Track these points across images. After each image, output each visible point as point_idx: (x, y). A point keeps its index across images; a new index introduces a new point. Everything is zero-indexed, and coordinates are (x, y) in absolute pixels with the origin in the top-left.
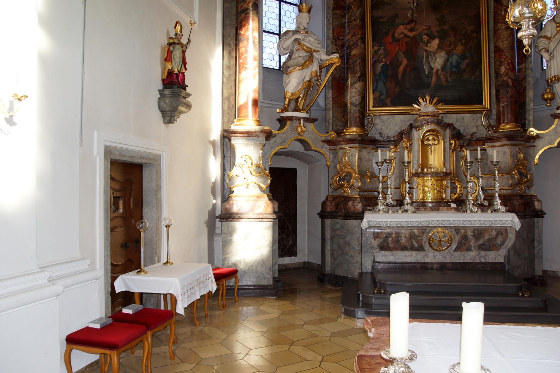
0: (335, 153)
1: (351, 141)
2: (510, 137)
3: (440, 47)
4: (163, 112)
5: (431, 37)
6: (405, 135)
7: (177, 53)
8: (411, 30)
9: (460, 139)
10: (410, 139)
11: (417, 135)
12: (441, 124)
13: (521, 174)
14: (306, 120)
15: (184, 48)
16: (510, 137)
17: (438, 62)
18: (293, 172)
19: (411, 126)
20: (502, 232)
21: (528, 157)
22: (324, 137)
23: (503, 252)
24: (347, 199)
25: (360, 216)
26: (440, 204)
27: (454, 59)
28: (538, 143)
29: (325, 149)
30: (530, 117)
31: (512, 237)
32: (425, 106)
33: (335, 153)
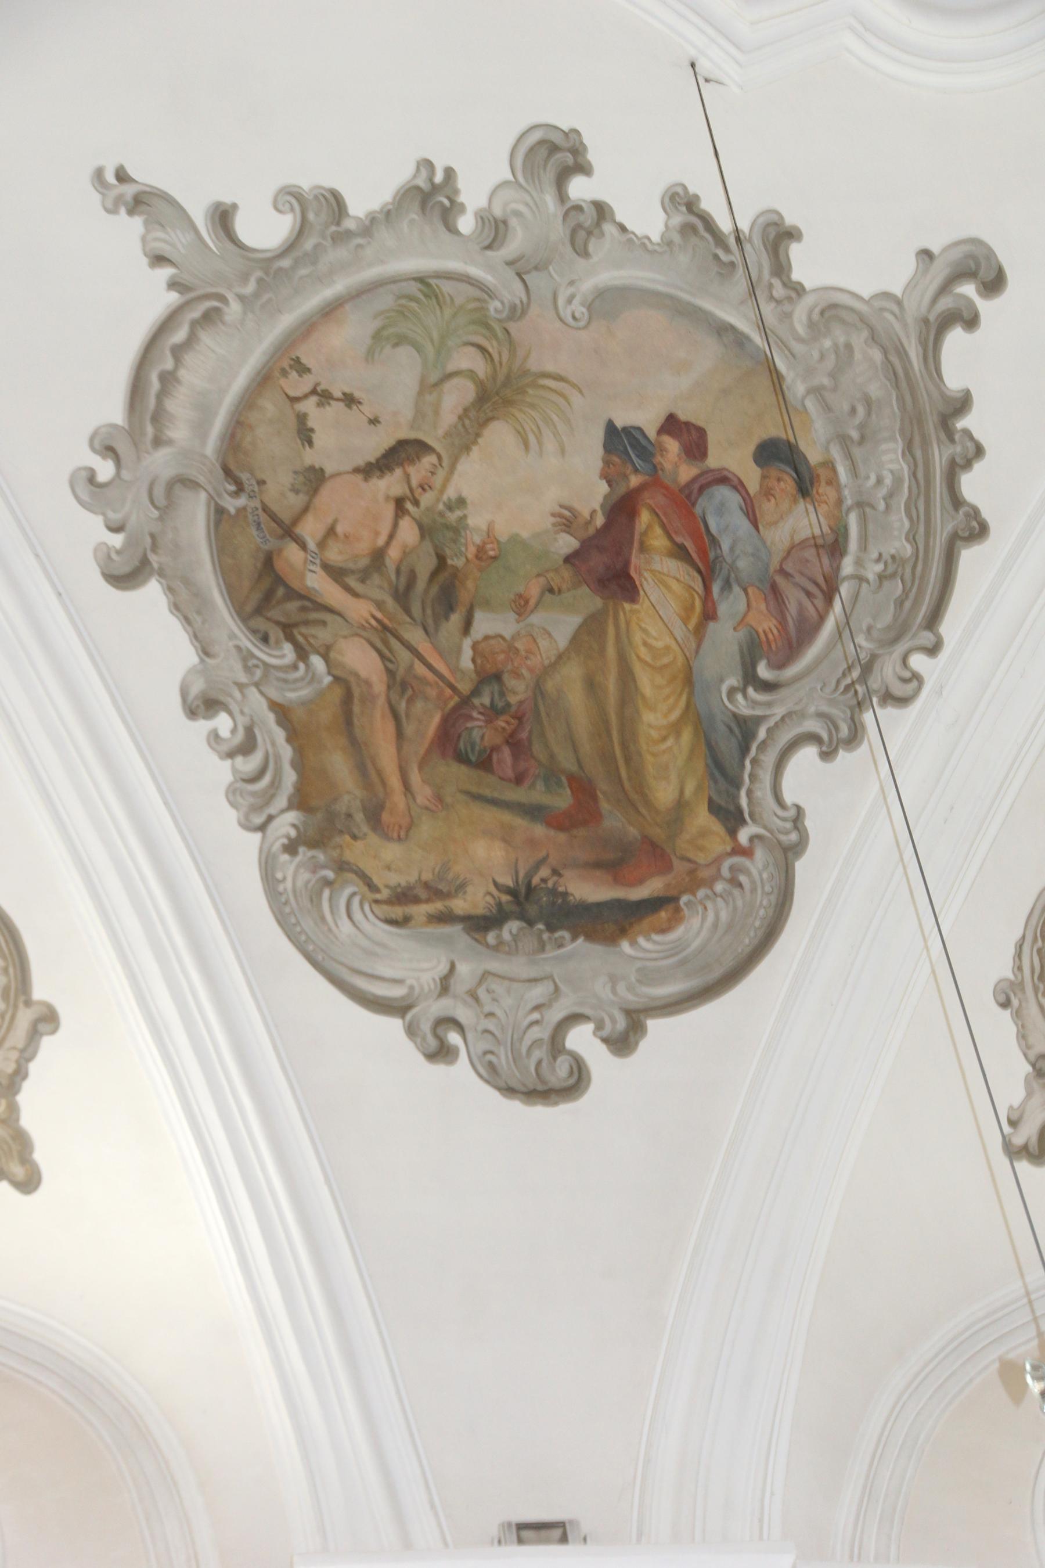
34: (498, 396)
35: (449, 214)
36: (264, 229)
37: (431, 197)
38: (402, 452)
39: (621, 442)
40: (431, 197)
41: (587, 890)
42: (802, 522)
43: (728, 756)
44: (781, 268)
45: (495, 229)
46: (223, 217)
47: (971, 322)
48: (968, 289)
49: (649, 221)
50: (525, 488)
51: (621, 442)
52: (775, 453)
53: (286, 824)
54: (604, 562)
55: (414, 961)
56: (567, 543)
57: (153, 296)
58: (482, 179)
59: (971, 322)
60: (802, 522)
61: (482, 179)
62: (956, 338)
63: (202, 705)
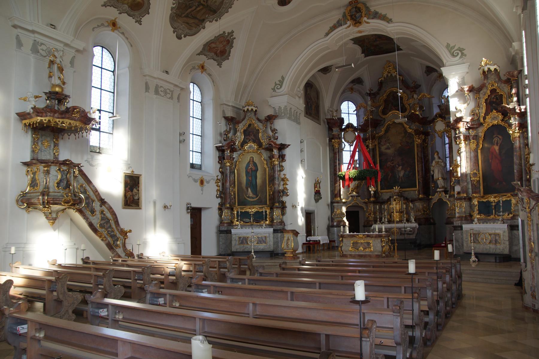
0: (367, 206)
1: (370, 203)
2: (420, 199)
3: (402, 169)
4: (315, 200)
5: (399, 166)
6: (389, 200)
7: (318, 185)
8: (393, 163)
9: (407, 200)
10: (390, 201)
11: (392, 199)
12: (400, 195)
13: (424, 211)
14: (357, 196)
15: (319, 183)
16: (420, 199)
17: (401, 174)
18: (358, 212)
19: (390, 197)
20: (414, 228)
21: (429, 205)
22: (363, 201)
23: (415, 235)
24: (370, 221)
25: (371, 226)
26: (401, 221)
27: (407, 173)
28: (432, 200)
29: (364, 206)
30: (431, 192)
31: (416, 230)
32: (396, 189)
33: (367, 206)
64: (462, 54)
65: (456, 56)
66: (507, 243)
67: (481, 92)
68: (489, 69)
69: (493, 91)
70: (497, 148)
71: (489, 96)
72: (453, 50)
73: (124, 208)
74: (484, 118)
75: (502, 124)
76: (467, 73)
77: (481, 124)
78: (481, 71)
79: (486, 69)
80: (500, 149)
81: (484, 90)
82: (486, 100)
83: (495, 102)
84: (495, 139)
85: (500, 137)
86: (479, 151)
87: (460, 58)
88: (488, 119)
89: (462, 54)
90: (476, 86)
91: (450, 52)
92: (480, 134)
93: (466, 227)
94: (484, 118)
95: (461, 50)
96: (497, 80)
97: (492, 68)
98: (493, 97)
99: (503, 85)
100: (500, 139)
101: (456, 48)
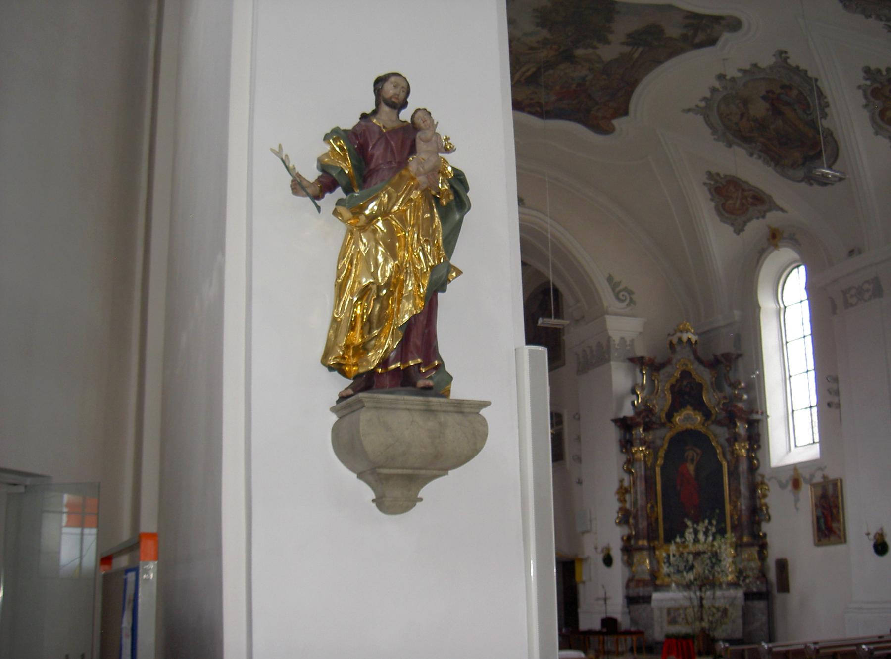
34: (746, 102)
35: (717, 90)
36: (703, 104)
37: (714, 90)
38: (742, 116)
39: (764, 98)
40: (714, 90)
41: (812, 153)
42: (795, 93)
43: (813, 125)
44: (759, 68)
45: (725, 88)
46: (697, 106)
47: (788, 58)
48: (783, 55)
49: (739, 75)
50: (760, 109)
51: (764, 98)
52: (783, 87)
53: (772, 164)
54: (776, 112)
55: (801, 173)
56: (770, 113)
57: (700, 118)
58: (717, 84)
59: (788, 58)
60: (795, 93)
61: (717, 84)
62: (788, 61)
63: (751, 155)
64: (631, 299)
65: (623, 301)
66: (740, 621)
67: (662, 372)
68: (689, 340)
69: (685, 374)
70: (691, 468)
71: (677, 381)
72: (618, 289)
73: (845, 541)
74: (670, 416)
75: (703, 430)
76: (640, 333)
77: (663, 425)
78: (675, 340)
79: (685, 337)
80: (697, 470)
81: (668, 369)
82: (672, 386)
83: (686, 393)
84: (690, 453)
85: (699, 451)
86: (658, 470)
87: (628, 305)
88: (677, 419)
89: (631, 299)
90: (659, 360)
91: (613, 289)
92: (659, 442)
93: (656, 596)
94: (670, 416)
95: (630, 292)
96: (692, 357)
97: (694, 338)
98: (685, 383)
99: (702, 368)
100: (698, 454)
101: (621, 287)
